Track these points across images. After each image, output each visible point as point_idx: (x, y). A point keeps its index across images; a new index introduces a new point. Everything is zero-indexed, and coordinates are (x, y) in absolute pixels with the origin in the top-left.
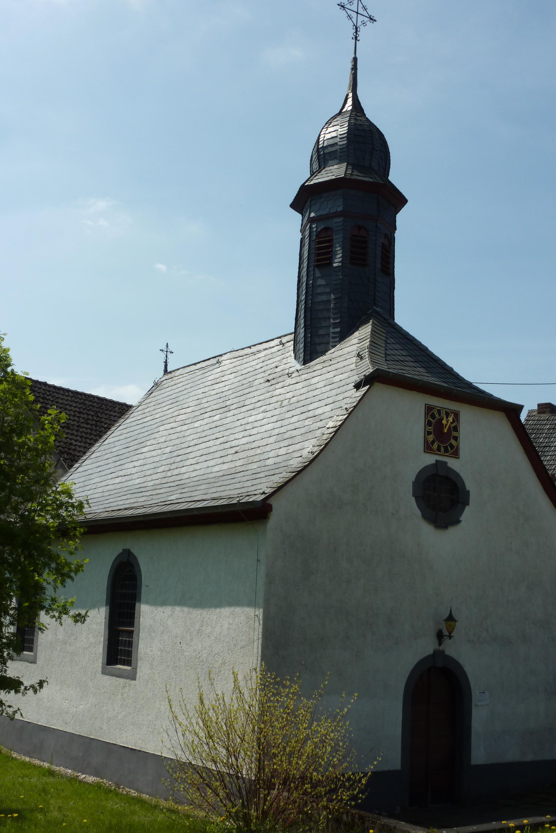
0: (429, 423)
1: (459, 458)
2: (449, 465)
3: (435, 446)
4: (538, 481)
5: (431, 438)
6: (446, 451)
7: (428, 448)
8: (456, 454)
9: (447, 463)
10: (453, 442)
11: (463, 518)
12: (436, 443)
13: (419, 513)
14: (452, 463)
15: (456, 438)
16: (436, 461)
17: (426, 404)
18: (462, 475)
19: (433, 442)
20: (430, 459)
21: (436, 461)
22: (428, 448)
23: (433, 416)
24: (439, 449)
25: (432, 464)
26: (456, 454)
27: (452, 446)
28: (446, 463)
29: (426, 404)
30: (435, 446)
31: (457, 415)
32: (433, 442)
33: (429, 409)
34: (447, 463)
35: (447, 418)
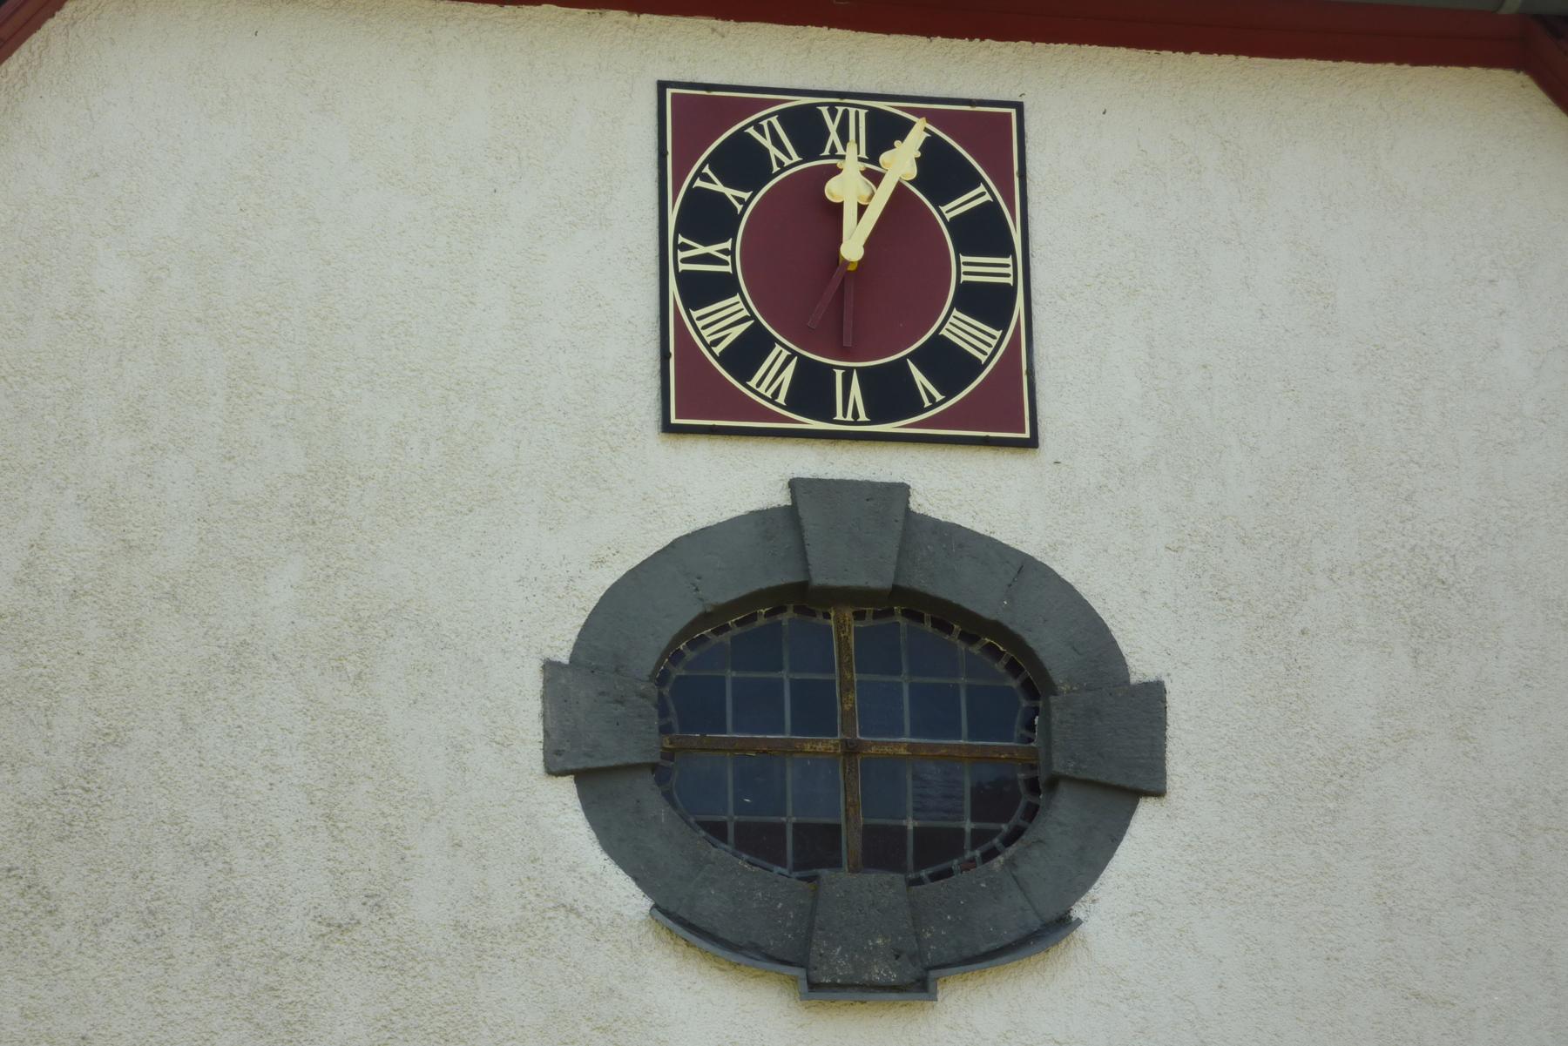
0: (704, 218)
1: (1032, 443)
2: (925, 502)
3: (774, 376)
4: (1347, 67)
5: (723, 322)
6: (888, 395)
7: (700, 397)
8: (999, 412)
9: (902, 490)
10: (961, 329)
11: (1104, 908)
12: (778, 354)
13: (626, 898)
14: (954, 486)
15: (991, 304)
16: (794, 485)
17: (662, 86)
18: (1068, 568)
19: (747, 354)
20: (741, 479)
21: (794, 485)
22: (700, 397)
23: (743, 163)
24: (812, 393)
25: (761, 519)
26: (999, 412)
27: (949, 365)
28: (900, 491)
29: (662, 86)
30: (774, 376)
31: (979, 145)
32: (747, 354)
33: (695, 119)
34: (902, 490)
35: (873, 154)
